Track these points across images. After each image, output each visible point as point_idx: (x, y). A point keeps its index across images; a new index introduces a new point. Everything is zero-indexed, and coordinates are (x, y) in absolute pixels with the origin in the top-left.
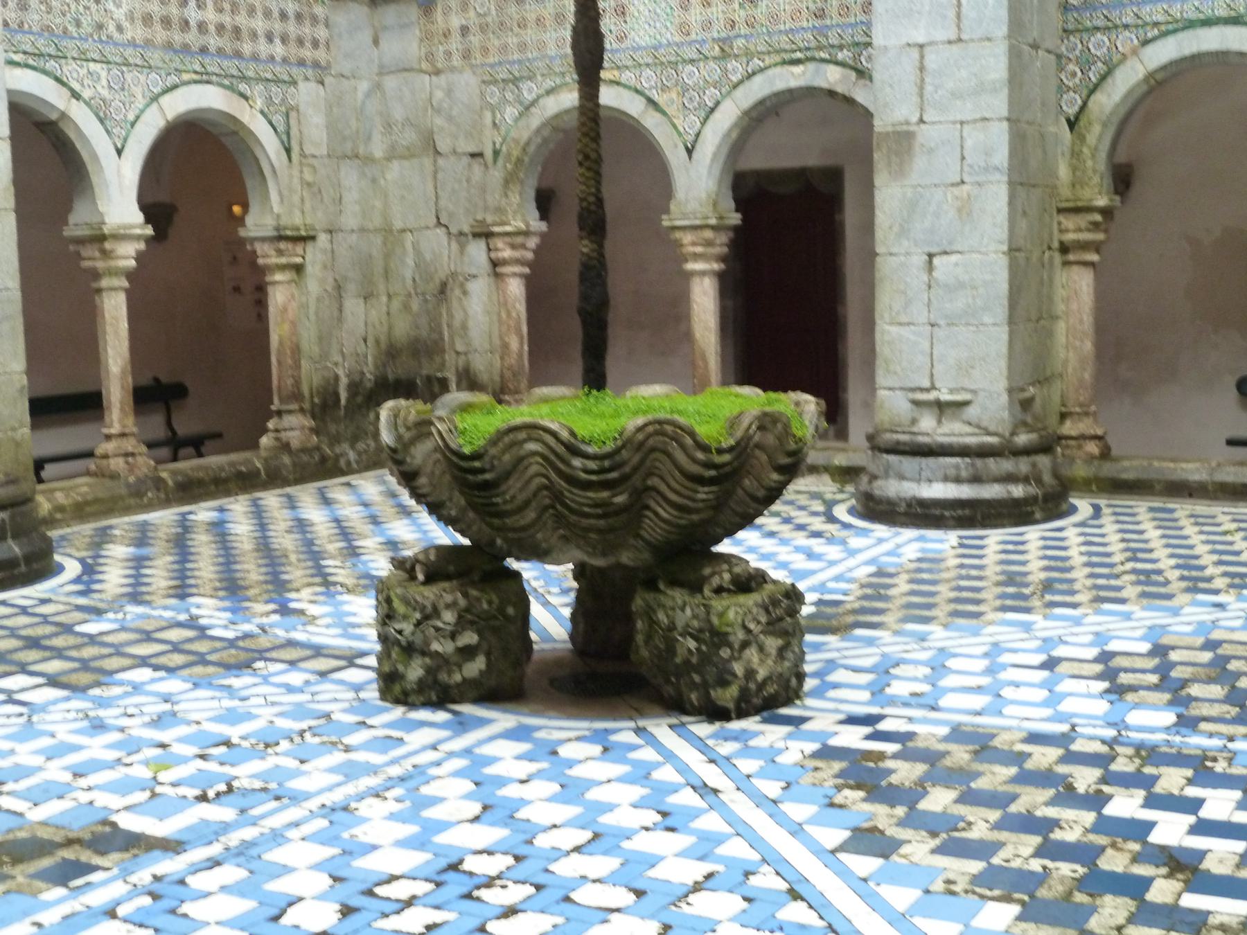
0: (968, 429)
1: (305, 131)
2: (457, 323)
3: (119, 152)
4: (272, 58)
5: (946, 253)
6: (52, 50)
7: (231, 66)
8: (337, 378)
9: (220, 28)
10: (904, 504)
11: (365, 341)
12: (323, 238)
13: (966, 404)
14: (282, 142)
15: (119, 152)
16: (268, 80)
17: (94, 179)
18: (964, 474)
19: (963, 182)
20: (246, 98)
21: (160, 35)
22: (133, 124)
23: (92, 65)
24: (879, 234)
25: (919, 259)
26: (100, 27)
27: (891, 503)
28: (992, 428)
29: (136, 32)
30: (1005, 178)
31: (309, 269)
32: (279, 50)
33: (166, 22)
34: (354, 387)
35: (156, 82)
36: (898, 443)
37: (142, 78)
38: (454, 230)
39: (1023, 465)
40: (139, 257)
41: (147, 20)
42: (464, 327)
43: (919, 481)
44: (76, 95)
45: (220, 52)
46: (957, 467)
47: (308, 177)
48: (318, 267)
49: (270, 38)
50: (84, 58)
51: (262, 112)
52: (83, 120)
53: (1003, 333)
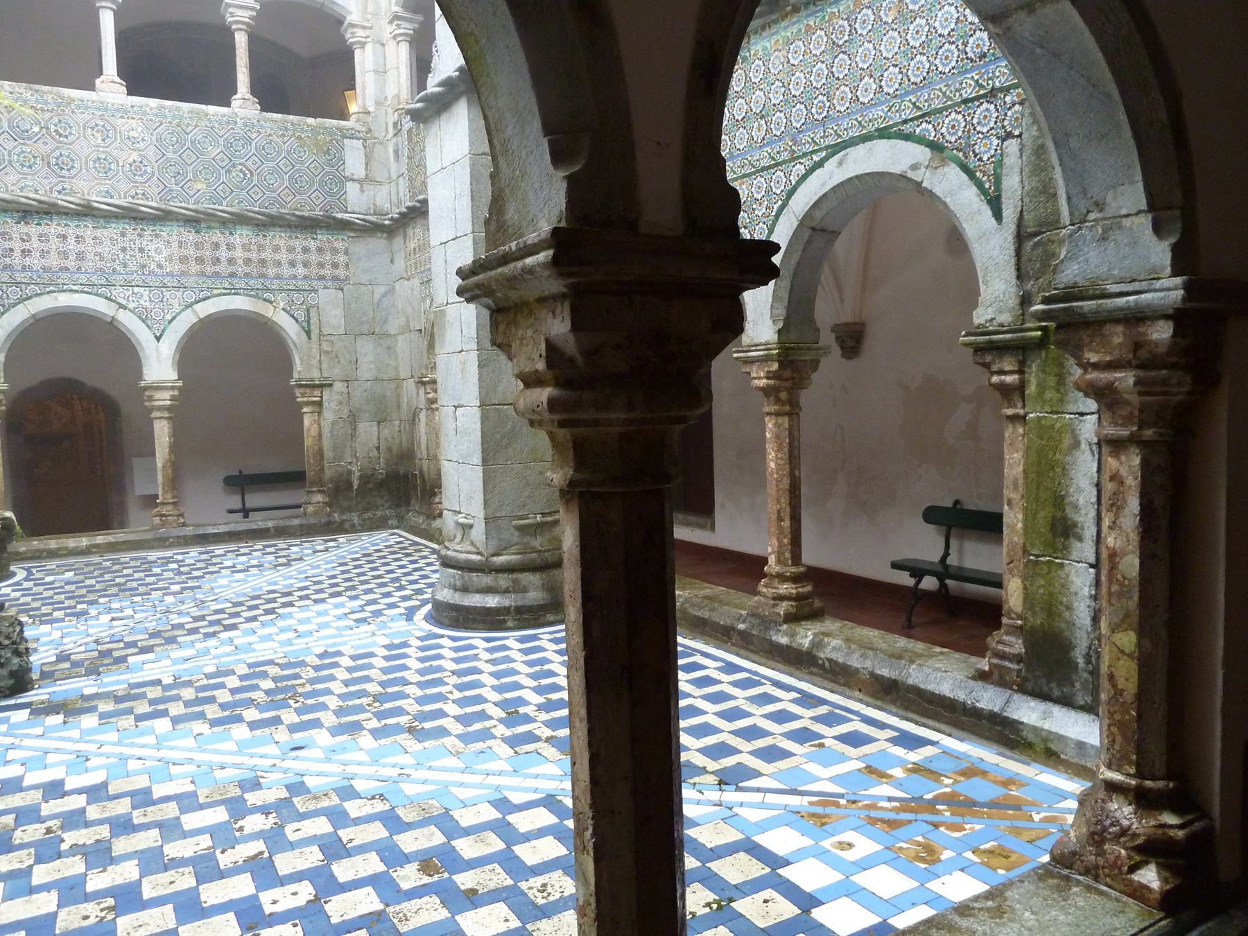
1: (324, 320)
3: (158, 339)
6: (103, 282)
7: (258, 284)
8: (350, 473)
11: (378, 448)
12: (339, 386)
13: (471, 526)
15: (158, 339)
17: (141, 355)
18: (458, 583)
20: (271, 303)
21: (195, 268)
22: (170, 322)
23: (136, 289)
26: (144, 266)
29: (176, 268)
31: (325, 404)
32: (301, 271)
33: (200, 260)
34: (365, 479)
35: (190, 296)
37: (179, 294)
39: (503, 580)
40: (173, 398)
41: (184, 260)
44: (121, 306)
45: (246, 275)
47: (325, 347)
48: (333, 405)
49: (292, 264)
50: (128, 285)
52: (130, 322)
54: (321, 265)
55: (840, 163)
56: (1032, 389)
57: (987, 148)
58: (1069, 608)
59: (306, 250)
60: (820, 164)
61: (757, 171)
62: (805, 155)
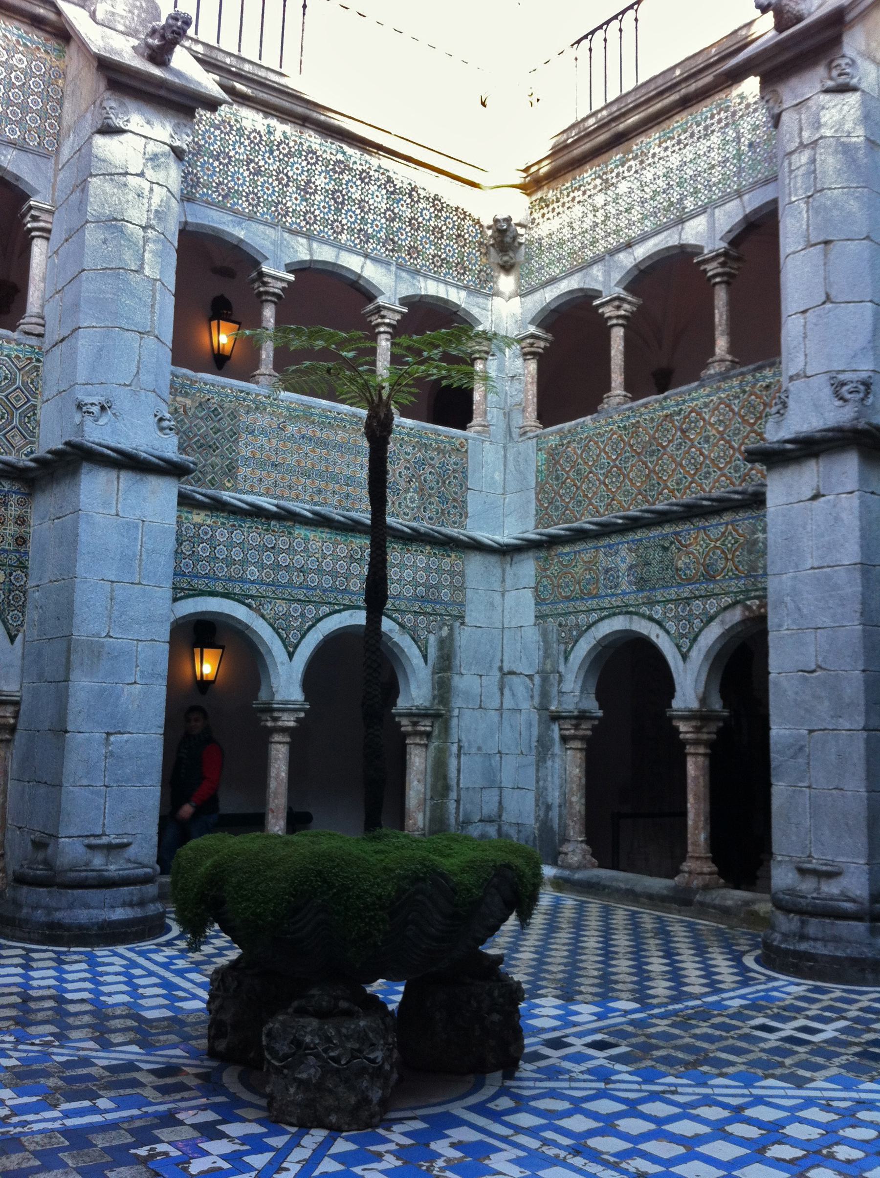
0: (130, 865)
5: (120, 733)
10: (96, 928)
19: (135, 683)
24: (71, 717)
25: (99, 736)
27: (81, 927)
30: (165, 683)
36: (87, 878)
43: (102, 908)
46: (131, 894)
53: (157, 791)
55: (351, 615)
56: (436, 732)
57: (423, 634)
58: (448, 819)
60: (339, 611)
62: (330, 603)
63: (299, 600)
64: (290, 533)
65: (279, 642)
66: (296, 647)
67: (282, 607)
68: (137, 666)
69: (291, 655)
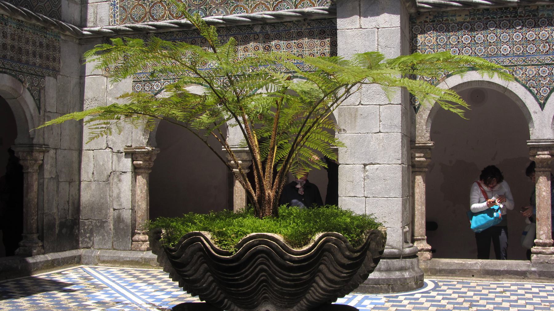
2: (115, 194)
4: (35, 64)
5: (372, 164)
9: (13, 47)
14: (37, 105)
16: (32, 74)
19: (380, 132)
20: (22, 82)
28: (395, 245)
32: (38, 61)
38: (115, 150)
42: (118, 197)
45: (12, 58)
51: (28, 89)
54: (48, 58)
59: (41, 44)
61: (543, 65)
63: (547, 64)
64: (534, 15)
65: (532, 97)
66: (547, 99)
67: (532, 71)
68: (380, 121)
69: (542, 106)
